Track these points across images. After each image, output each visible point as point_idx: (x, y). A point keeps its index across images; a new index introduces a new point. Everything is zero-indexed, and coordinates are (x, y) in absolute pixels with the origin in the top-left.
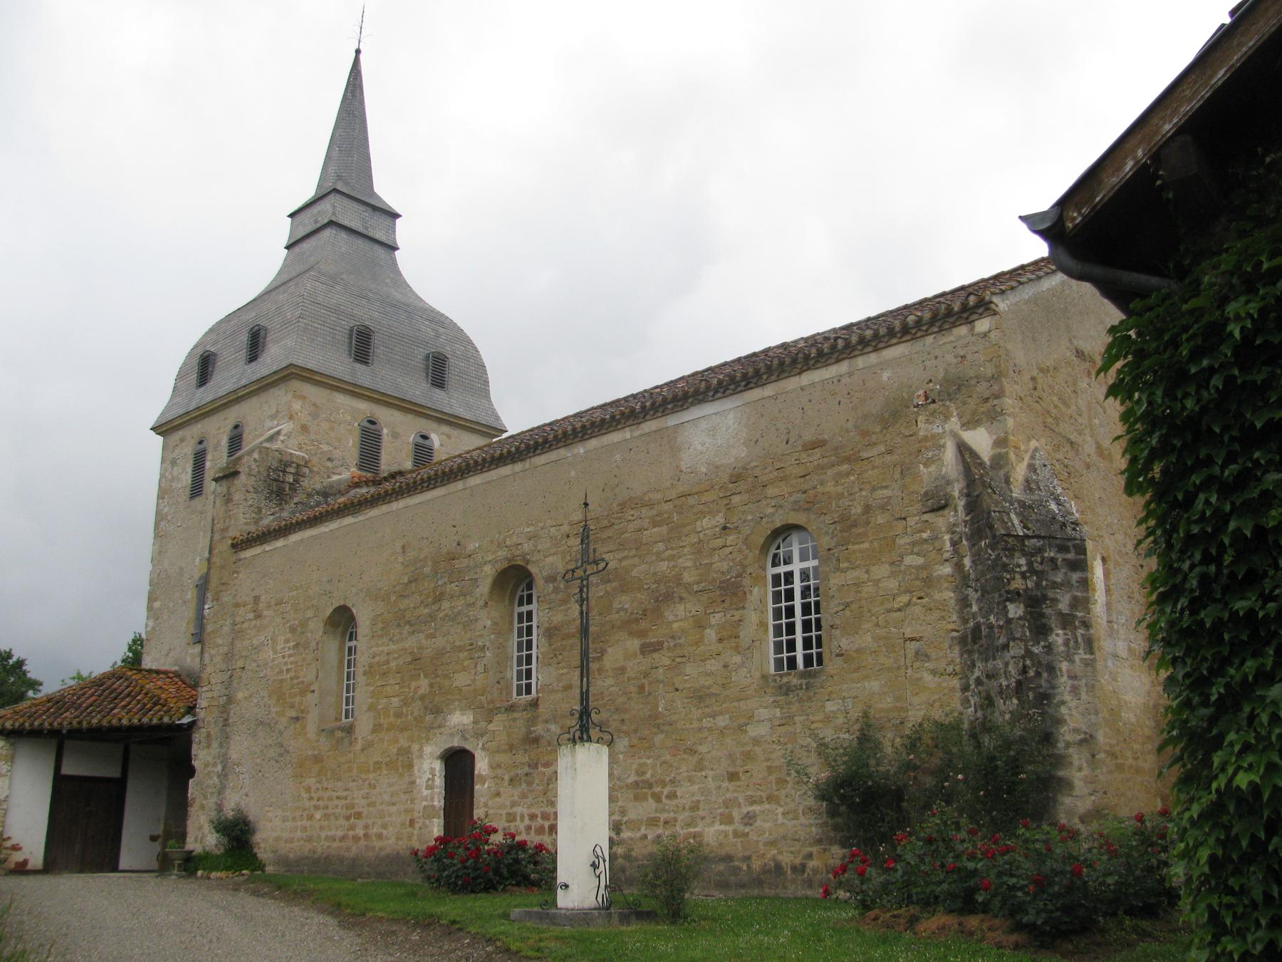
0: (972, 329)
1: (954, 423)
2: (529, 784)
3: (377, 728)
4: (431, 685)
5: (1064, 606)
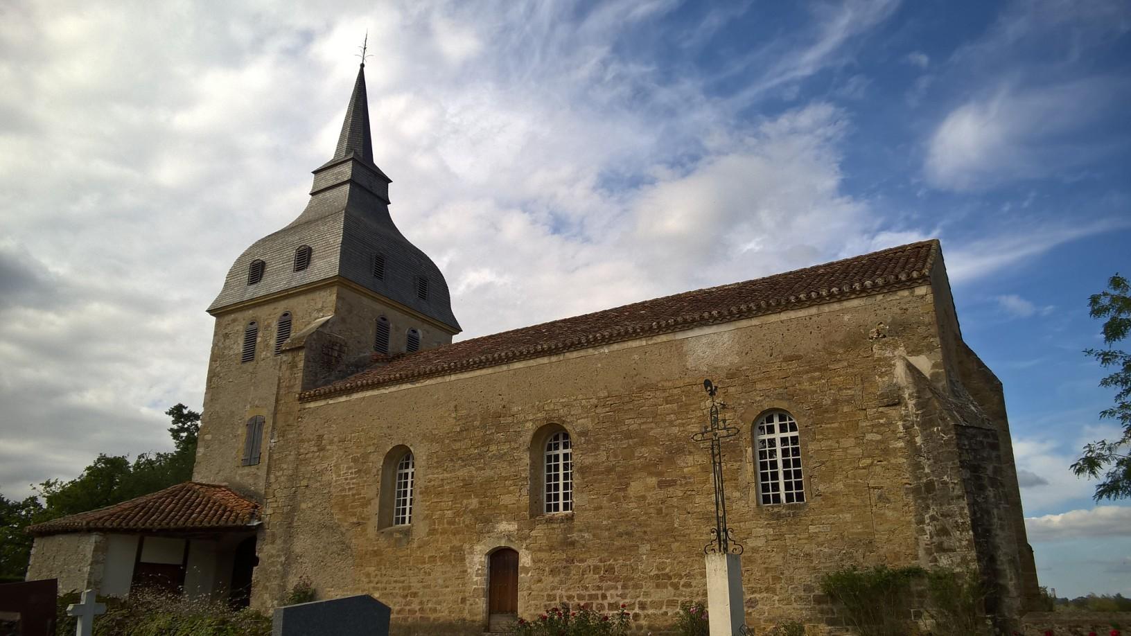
0: (912, 293)
1: (901, 351)
2: (568, 574)
3: (432, 532)
4: (481, 503)
5: (990, 471)
